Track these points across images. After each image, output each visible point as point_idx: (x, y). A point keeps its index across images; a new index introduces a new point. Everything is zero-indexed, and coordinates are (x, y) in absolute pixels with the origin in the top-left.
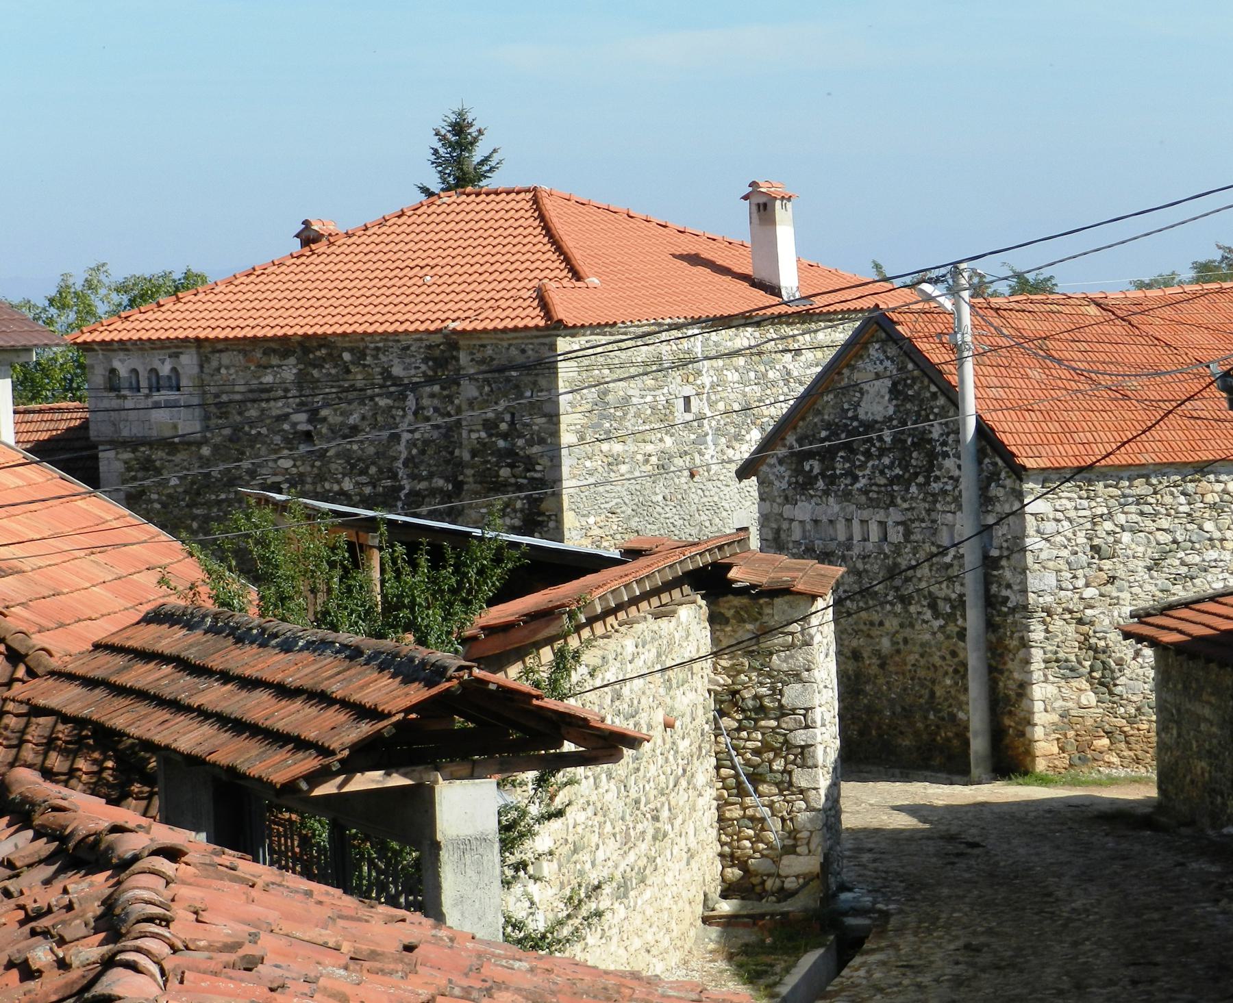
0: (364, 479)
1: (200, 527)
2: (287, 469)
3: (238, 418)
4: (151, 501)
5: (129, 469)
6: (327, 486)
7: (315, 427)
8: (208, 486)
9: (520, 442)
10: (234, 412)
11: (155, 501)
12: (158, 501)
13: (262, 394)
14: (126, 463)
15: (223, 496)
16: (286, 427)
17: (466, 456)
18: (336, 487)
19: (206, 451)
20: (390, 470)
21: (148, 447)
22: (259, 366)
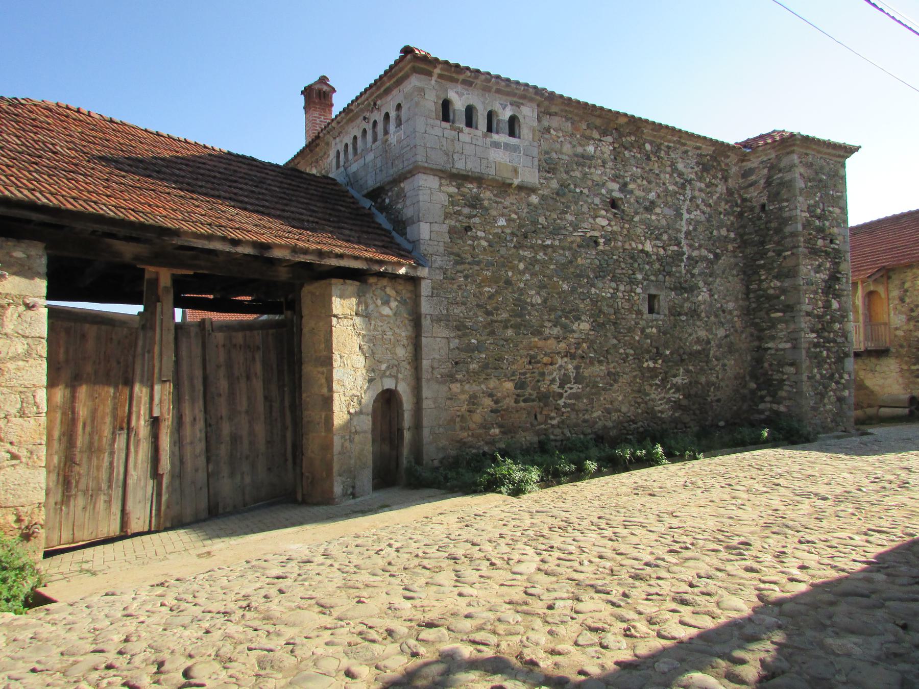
0: (659, 243)
1: (526, 268)
2: (603, 227)
3: (565, 176)
4: (476, 238)
5: (452, 204)
6: (634, 245)
7: (625, 196)
8: (534, 232)
9: (827, 223)
10: (562, 169)
11: (481, 238)
12: (484, 238)
13: (584, 160)
14: (450, 196)
15: (548, 242)
16: (603, 191)
17: (800, 228)
18: (640, 247)
19: (534, 199)
20: (676, 239)
21: (475, 185)
22: (583, 136)
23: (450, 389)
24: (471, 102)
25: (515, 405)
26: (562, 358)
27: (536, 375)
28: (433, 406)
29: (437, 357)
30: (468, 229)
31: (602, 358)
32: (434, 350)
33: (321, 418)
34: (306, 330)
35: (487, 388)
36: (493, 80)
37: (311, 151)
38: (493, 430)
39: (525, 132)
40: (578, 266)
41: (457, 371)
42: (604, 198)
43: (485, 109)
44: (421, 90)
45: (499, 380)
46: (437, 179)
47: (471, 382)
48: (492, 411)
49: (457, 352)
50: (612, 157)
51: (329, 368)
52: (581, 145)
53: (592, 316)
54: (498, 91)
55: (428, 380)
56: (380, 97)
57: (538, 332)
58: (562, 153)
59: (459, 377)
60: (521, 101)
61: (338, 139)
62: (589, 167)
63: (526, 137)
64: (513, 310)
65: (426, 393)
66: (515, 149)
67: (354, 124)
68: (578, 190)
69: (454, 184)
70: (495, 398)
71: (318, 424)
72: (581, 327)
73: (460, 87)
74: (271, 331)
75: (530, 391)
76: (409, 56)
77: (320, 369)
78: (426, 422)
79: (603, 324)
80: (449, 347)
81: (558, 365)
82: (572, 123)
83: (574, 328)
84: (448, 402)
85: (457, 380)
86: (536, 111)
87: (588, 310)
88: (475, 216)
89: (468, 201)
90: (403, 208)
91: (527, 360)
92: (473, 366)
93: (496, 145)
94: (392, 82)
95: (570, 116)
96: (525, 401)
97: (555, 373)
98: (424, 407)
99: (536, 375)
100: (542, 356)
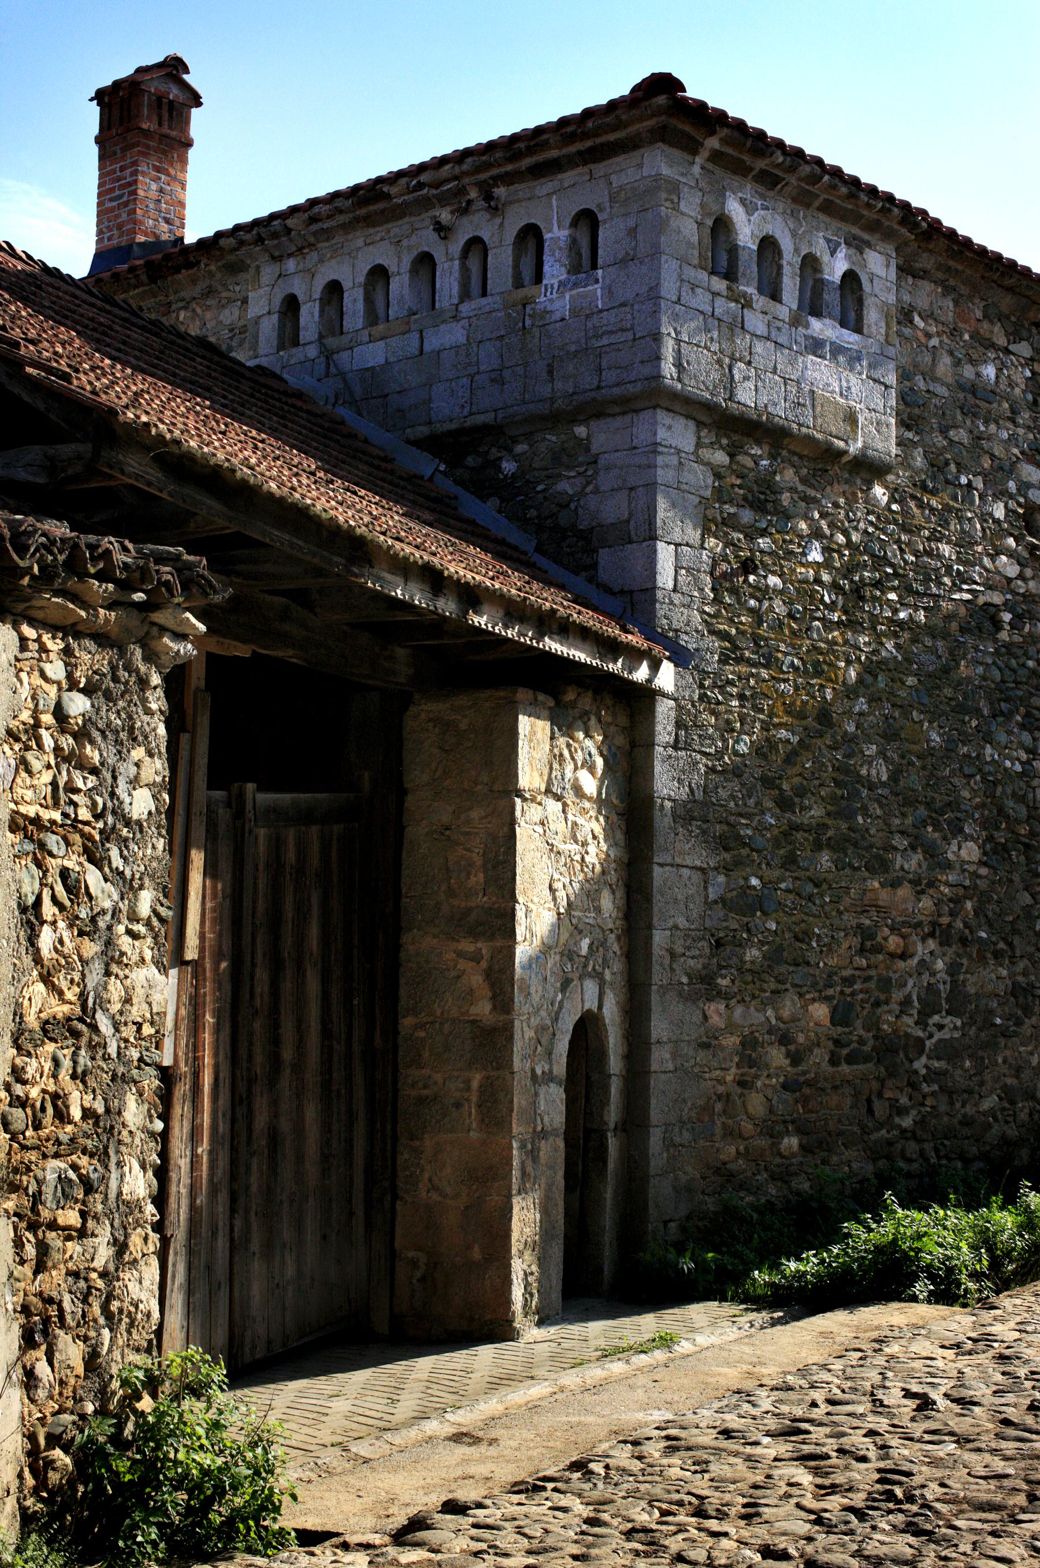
3: (940, 441)
4: (763, 592)
5: (720, 495)
21: (766, 448)
22: (975, 336)
23: (706, 1017)
24: (769, 229)
25: (830, 1069)
26: (923, 940)
27: (872, 985)
28: (671, 1067)
29: (682, 922)
30: (748, 566)
31: (1001, 945)
32: (676, 901)
33: (468, 1089)
34: (417, 831)
35: (778, 1018)
36: (826, 178)
37: (153, 280)
38: (786, 1140)
39: (872, 316)
40: (960, 684)
41: (721, 967)
42: (1012, 504)
43: (797, 250)
44: (674, 188)
45: (801, 995)
46: (691, 424)
47: (747, 999)
48: (785, 1087)
49: (719, 912)
50: (1030, 397)
51: (499, 943)
52: (973, 362)
53: (984, 826)
54: (828, 208)
55: (664, 990)
56: (508, 179)
57: (879, 865)
58: (935, 379)
59: (723, 982)
60: (866, 236)
61: (291, 265)
62: (986, 422)
63: (874, 329)
64: (834, 799)
65: (659, 1027)
66: (854, 359)
67: (379, 232)
68: (964, 480)
69: (725, 441)
70: (792, 1047)
71: (458, 1105)
72: (963, 853)
73: (748, 191)
74: (337, 829)
75: (862, 1032)
76: (661, 100)
77: (467, 946)
78: (657, 1111)
79: (1005, 848)
80: (707, 897)
81: (915, 961)
82: (956, 303)
83: (950, 856)
84: (702, 1054)
85: (719, 993)
86: (893, 263)
87: (977, 807)
88: (764, 532)
89: (751, 491)
90: (582, 493)
91: (855, 942)
92: (752, 954)
93: (815, 346)
94: (572, 149)
95: (952, 282)
96: (851, 1060)
97: (910, 983)
98: (653, 1069)
99: (872, 985)
100: (886, 931)
